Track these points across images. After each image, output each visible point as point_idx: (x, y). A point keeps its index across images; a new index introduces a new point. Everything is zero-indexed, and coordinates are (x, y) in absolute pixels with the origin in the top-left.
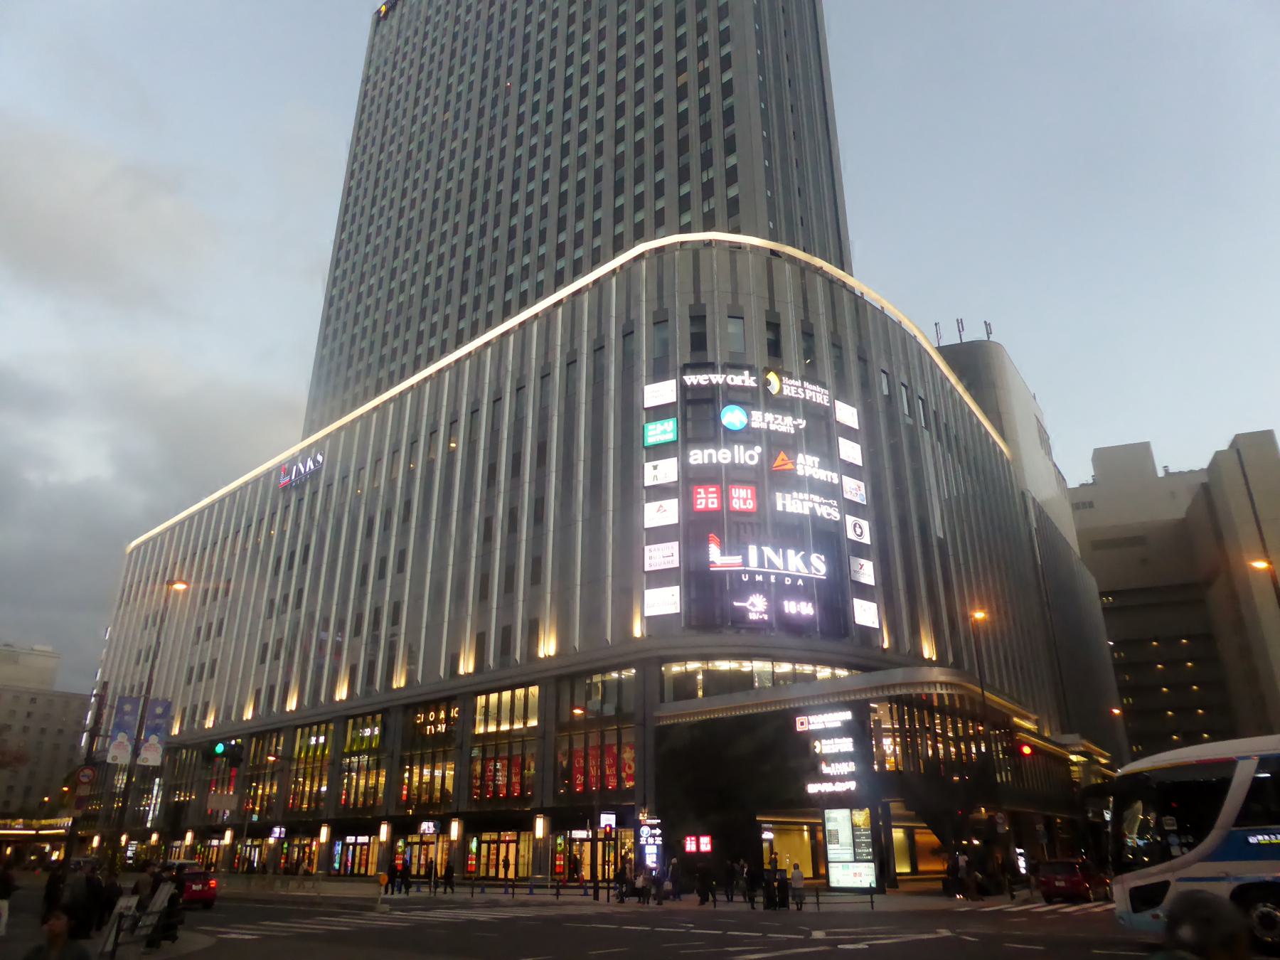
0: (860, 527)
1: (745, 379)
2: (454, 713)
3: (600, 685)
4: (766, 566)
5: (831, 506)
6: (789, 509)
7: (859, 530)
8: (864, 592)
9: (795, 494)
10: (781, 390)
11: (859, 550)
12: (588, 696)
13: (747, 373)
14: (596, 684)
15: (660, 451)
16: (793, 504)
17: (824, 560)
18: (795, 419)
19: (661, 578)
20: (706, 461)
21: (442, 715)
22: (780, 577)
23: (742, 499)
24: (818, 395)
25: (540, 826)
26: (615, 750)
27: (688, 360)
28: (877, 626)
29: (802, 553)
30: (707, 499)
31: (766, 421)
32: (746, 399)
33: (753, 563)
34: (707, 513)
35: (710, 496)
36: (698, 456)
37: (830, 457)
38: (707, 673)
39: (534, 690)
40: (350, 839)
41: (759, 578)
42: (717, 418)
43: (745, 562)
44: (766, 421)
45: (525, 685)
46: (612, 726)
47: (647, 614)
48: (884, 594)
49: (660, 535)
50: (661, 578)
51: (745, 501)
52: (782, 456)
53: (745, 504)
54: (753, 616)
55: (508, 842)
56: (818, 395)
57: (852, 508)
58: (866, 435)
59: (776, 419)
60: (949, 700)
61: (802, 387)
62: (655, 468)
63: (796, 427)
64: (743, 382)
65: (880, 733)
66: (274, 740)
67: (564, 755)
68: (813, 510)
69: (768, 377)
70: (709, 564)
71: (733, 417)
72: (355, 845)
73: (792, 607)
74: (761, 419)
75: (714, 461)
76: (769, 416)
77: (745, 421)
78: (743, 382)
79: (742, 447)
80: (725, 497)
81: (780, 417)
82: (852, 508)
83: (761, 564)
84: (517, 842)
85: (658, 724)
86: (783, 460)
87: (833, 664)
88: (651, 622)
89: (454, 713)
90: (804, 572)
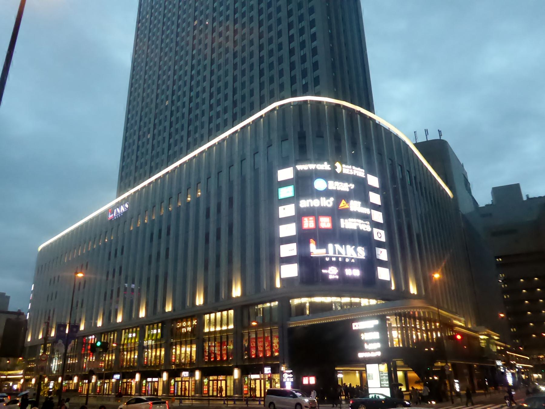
0: (380, 234)
1: (325, 166)
2: (195, 322)
3: (261, 309)
4: (337, 253)
5: (366, 224)
6: (347, 227)
7: (380, 235)
8: (382, 264)
9: (350, 219)
10: (342, 171)
11: (380, 245)
12: (256, 314)
13: (326, 163)
14: (260, 309)
15: (286, 201)
16: (348, 224)
17: (364, 250)
18: (349, 184)
19: (288, 260)
20: (308, 206)
21: (189, 323)
22: (344, 258)
23: (325, 223)
24: (360, 172)
25: (236, 373)
26: (270, 339)
27: (298, 158)
28: (389, 279)
29: (354, 247)
30: (309, 223)
31: (335, 186)
33: (331, 253)
35: (310, 221)
36: (304, 203)
37: (366, 202)
38: (311, 304)
39: (231, 312)
40: (149, 379)
41: (334, 259)
42: (313, 185)
43: (327, 253)
44: (335, 186)
45: (227, 310)
46: (268, 328)
47: (282, 277)
48: (392, 264)
49: (288, 240)
50: (288, 260)
51: (326, 223)
52: (343, 202)
53: (326, 225)
54: (331, 277)
56: (360, 172)
58: (382, 190)
59: (340, 185)
60: (423, 314)
61: (352, 169)
62: (284, 209)
63: (349, 188)
64: (324, 168)
65: (391, 328)
68: (358, 227)
69: (335, 165)
70: (310, 253)
71: (320, 184)
72: (152, 382)
73: (349, 272)
74: (334, 185)
75: (312, 206)
76: (337, 183)
77: (326, 186)
78: (324, 168)
79: (324, 198)
80: (317, 222)
81: (341, 183)
83: (335, 253)
84: (226, 380)
85: (288, 327)
86: (344, 204)
87: (369, 298)
89: (195, 322)
90: (355, 256)
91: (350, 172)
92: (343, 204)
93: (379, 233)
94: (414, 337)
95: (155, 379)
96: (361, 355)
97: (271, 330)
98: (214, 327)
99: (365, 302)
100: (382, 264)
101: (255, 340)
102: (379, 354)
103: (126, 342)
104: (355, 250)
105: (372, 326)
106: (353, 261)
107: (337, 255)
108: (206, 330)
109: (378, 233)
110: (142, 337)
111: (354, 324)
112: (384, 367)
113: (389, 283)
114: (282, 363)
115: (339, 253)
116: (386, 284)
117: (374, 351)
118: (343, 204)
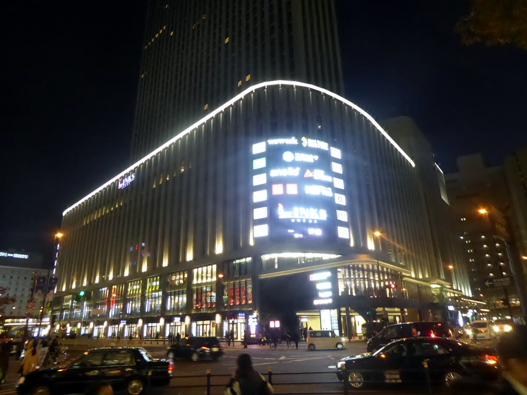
1: (293, 141)
2: (186, 276)
5: (328, 190)
7: (341, 200)
8: (342, 224)
11: (341, 208)
13: (293, 138)
15: (260, 171)
16: (312, 190)
19: (261, 222)
21: (182, 276)
23: (292, 189)
28: (348, 238)
29: (317, 210)
32: (293, 149)
34: (278, 196)
36: (275, 173)
37: (329, 171)
38: (279, 259)
40: (150, 325)
47: (255, 236)
48: (352, 224)
49: (260, 205)
50: (261, 222)
52: (308, 171)
55: (207, 325)
56: (323, 145)
57: (338, 191)
63: (314, 159)
66: (121, 287)
67: (226, 291)
71: (287, 156)
72: (152, 327)
78: (292, 142)
82: (338, 191)
83: (300, 215)
84: (210, 324)
86: (308, 173)
88: (256, 240)
91: (314, 145)
92: (308, 174)
93: (340, 198)
94: (362, 285)
95: (154, 324)
96: (316, 302)
97: (246, 281)
98: (201, 279)
99: (326, 256)
100: (342, 224)
101: (233, 291)
102: (330, 301)
103: (131, 293)
104: (318, 212)
105: (325, 278)
106: (315, 222)
107: (302, 217)
108: (195, 282)
109: (339, 198)
110: (144, 287)
111: (311, 276)
112: (334, 312)
113: (348, 241)
114: (254, 310)
115: (304, 216)
116: (346, 242)
117: (327, 298)
118: (308, 174)
